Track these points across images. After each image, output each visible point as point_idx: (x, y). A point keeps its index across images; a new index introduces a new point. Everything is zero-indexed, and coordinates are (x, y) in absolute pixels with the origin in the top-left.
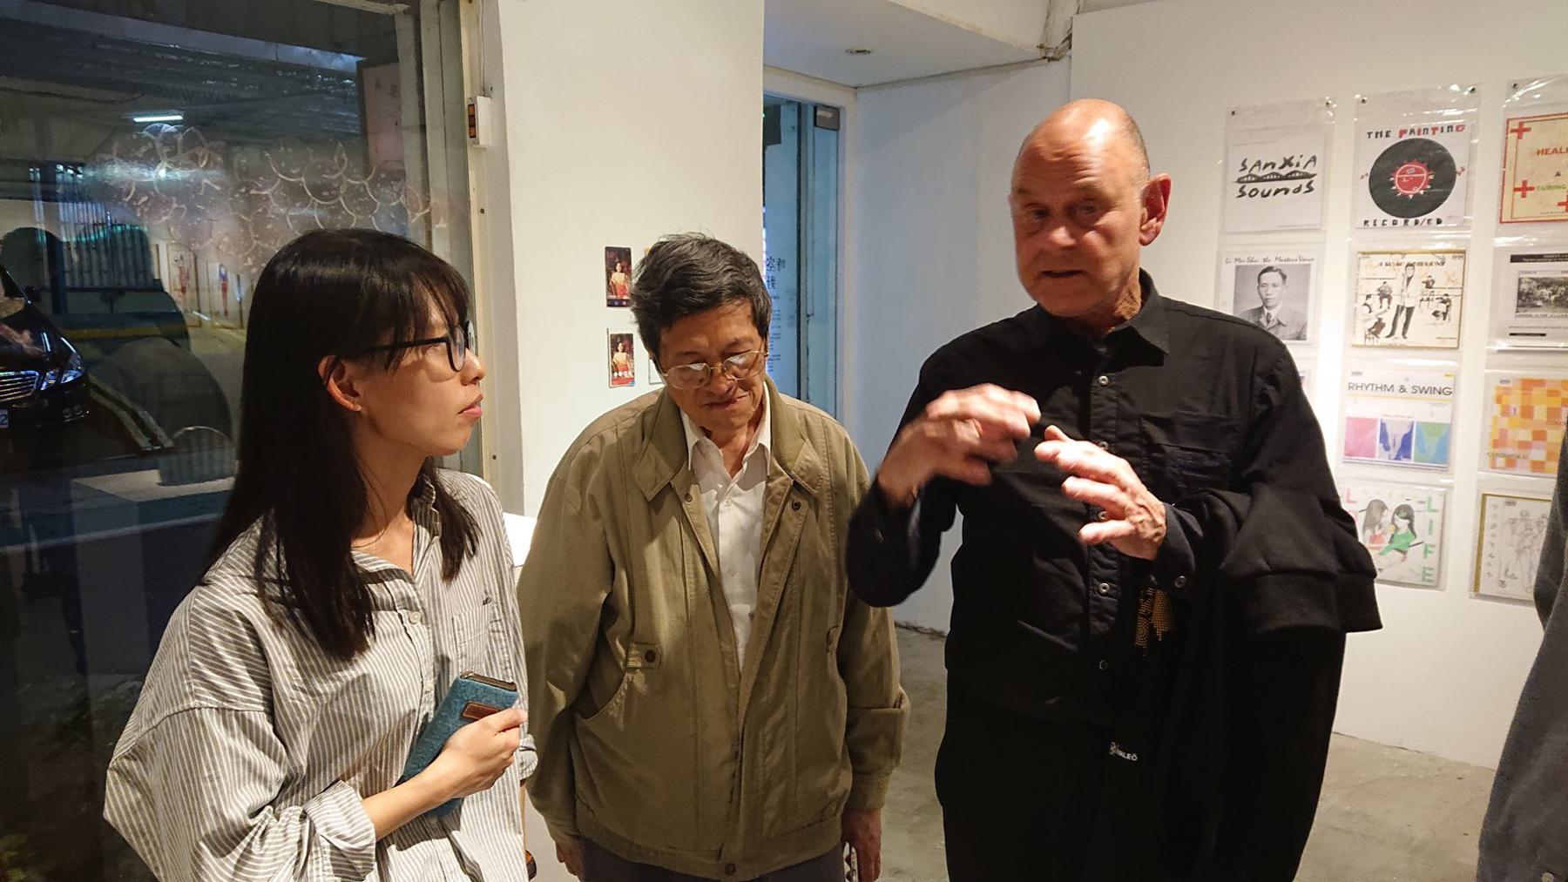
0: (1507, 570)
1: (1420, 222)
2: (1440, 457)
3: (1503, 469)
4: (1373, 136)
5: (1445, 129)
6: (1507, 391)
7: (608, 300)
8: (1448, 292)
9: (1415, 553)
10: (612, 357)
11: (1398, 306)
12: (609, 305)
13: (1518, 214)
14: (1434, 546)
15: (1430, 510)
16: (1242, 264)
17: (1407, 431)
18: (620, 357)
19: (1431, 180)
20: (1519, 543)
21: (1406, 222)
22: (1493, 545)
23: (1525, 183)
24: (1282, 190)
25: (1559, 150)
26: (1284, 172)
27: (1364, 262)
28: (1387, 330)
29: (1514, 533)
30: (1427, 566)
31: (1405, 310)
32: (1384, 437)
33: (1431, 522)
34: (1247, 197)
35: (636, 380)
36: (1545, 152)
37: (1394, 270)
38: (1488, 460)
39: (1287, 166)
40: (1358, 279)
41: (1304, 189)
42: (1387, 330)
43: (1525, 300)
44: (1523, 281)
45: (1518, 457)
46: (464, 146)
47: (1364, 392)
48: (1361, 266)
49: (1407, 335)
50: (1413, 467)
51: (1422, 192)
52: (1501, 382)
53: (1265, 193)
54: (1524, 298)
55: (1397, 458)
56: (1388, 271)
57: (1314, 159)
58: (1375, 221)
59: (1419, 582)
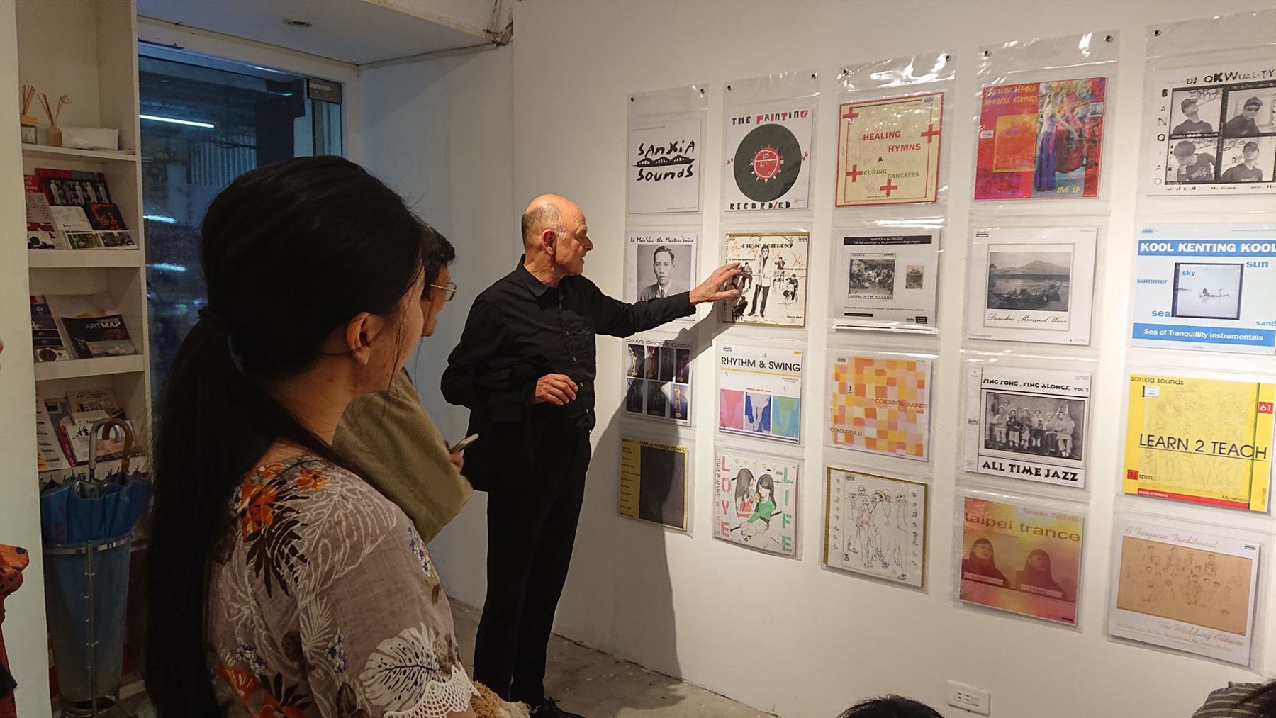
0: (849, 545)
2: (794, 434)
4: (737, 121)
5: (793, 115)
6: (844, 369)
11: (757, 285)
13: (852, 198)
16: (642, 243)
17: (766, 404)
20: (858, 518)
21: (763, 205)
23: (855, 167)
24: (669, 174)
26: (671, 157)
27: (731, 243)
31: (762, 289)
33: (787, 492)
36: (869, 137)
37: (753, 251)
38: (831, 437)
39: (673, 151)
41: (686, 173)
42: (748, 309)
43: (856, 281)
44: (854, 263)
50: (770, 439)
52: (839, 360)
53: (658, 177)
54: (854, 280)
57: (693, 143)
58: (739, 204)
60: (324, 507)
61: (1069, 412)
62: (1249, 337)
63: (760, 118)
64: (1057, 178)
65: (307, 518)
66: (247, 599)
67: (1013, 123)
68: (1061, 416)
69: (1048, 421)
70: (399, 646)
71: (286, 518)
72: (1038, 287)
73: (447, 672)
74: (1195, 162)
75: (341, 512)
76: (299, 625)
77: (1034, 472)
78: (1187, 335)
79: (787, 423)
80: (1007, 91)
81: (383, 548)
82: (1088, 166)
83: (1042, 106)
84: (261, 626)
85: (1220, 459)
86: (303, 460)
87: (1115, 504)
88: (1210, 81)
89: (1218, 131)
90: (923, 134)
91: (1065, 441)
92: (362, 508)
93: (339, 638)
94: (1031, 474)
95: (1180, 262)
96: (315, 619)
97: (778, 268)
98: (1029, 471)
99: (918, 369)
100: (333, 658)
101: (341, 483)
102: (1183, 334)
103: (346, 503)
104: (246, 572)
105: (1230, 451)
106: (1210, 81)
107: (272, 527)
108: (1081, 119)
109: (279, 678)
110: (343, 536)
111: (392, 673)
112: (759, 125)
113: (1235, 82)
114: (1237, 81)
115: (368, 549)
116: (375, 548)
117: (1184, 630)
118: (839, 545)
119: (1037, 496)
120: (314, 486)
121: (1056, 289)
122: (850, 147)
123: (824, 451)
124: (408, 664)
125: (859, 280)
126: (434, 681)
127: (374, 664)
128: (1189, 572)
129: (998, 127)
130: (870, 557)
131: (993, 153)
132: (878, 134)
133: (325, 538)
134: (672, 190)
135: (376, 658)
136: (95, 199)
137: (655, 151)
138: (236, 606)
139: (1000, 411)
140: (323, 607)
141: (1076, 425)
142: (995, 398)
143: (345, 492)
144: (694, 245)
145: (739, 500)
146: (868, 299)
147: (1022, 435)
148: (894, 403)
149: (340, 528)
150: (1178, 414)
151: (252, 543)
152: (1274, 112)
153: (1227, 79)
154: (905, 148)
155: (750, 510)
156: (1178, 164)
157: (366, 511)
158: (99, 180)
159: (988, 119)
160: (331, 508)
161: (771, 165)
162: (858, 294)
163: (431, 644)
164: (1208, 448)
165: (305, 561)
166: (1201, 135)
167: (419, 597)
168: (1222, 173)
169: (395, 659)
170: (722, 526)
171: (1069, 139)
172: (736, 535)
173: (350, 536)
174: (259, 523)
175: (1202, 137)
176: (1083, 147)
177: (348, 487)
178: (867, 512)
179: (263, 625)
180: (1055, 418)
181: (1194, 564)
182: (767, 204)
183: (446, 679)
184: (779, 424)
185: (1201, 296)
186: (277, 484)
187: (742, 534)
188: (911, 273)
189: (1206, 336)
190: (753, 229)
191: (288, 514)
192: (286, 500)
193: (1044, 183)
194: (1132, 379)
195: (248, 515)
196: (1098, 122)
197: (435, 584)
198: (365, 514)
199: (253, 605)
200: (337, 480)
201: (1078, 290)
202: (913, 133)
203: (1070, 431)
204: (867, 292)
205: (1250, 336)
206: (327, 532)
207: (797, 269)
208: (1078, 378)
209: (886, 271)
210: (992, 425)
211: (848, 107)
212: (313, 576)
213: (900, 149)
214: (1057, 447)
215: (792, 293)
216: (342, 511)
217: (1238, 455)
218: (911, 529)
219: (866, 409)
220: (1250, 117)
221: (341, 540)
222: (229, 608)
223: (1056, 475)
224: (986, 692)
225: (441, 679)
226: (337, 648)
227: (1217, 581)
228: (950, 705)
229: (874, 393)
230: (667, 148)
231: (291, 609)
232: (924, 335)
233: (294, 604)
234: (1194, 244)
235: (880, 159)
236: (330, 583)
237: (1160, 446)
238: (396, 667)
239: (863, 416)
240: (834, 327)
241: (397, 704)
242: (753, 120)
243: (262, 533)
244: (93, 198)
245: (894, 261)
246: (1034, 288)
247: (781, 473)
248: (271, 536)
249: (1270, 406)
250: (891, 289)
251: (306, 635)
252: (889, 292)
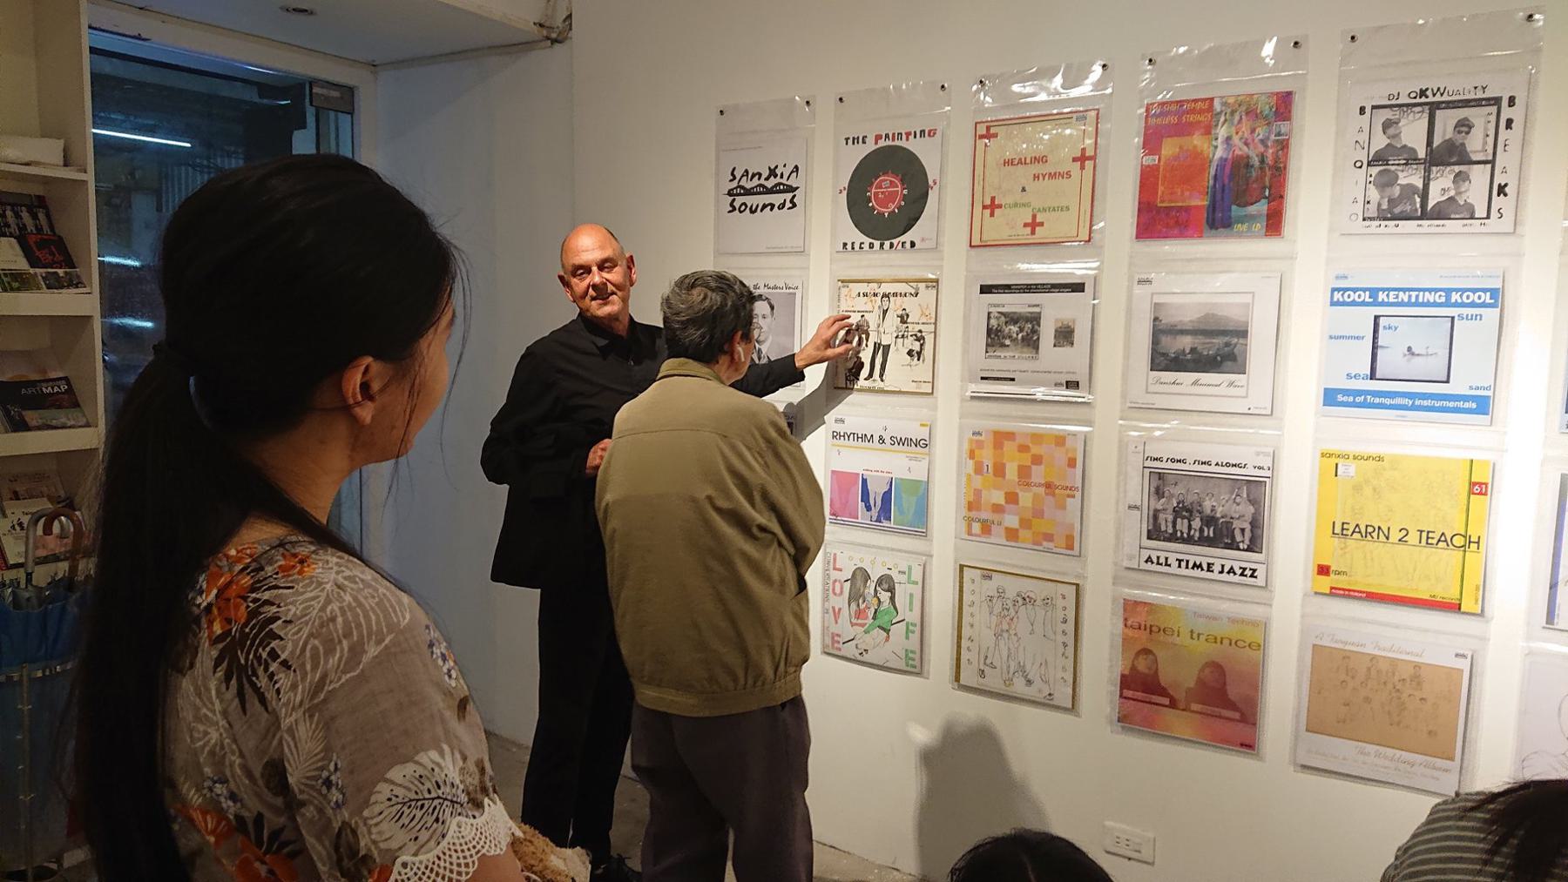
0: (986, 659)
2: (919, 524)
3: (979, 536)
4: (850, 141)
5: (918, 135)
6: (980, 445)
9: (898, 631)
11: (875, 343)
13: (989, 236)
14: (915, 625)
21: (882, 245)
23: (993, 199)
25: (1023, 160)
26: (769, 184)
27: (844, 291)
30: (910, 648)
33: (911, 595)
36: (1009, 163)
37: (871, 301)
38: (964, 529)
41: (788, 205)
42: (865, 372)
43: (995, 338)
44: (992, 315)
48: (842, 296)
53: (754, 208)
54: (993, 336)
55: (878, 520)
57: (796, 167)
58: (853, 243)
59: (902, 665)
60: (313, 599)
61: (1248, 495)
62: (1460, 404)
63: (878, 138)
64: (1233, 214)
65: (292, 613)
66: (215, 718)
67: (1181, 148)
68: (1238, 499)
69: (1223, 506)
70: (415, 774)
71: (264, 613)
72: (1210, 345)
73: (479, 805)
74: (1397, 195)
75: (335, 606)
76: (283, 750)
77: (1205, 567)
78: (1388, 401)
79: (912, 510)
80: (1174, 108)
81: (393, 650)
82: (1270, 199)
83: (1217, 125)
84: (233, 753)
85: (1427, 550)
86: (286, 541)
87: (1303, 606)
88: (1415, 98)
89: (1424, 157)
90: (1075, 160)
91: (1243, 530)
92: (362, 600)
93: (336, 765)
94: (1202, 570)
95: (1381, 314)
96: (303, 742)
97: (901, 322)
98: (1200, 566)
99: (1069, 443)
100: (328, 792)
101: (335, 568)
102: (1383, 400)
103: (342, 594)
104: (213, 685)
105: (1439, 541)
106: (1415, 98)
107: (246, 625)
108: (1263, 142)
109: (259, 818)
110: (338, 636)
111: (405, 808)
112: (875, 147)
113: (1443, 99)
114: (1445, 98)
115: (372, 651)
116: (381, 651)
117: (1386, 757)
118: (973, 656)
119: (1211, 597)
120: (300, 573)
121: (1232, 347)
122: (987, 174)
123: (955, 544)
124: (427, 796)
125: (998, 337)
126: (460, 818)
127: (382, 797)
128: (1392, 686)
129: (1163, 152)
130: (1011, 673)
131: (1158, 184)
132: (1020, 159)
133: (315, 638)
134: (769, 226)
135: (384, 790)
136: (34, 229)
137: (750, 176)
138: (201, 728)
139: (1166, 495)
140: (313, 726)
141: (1256, 509)
142: (1160, 479)
143: (342, 580)
145: (854, 606)
147: (1192, 523)
148: (1040, 485)
149: (335, 625)
150: (1377, 497)
151: (221, 646)
152: (1487, 136)
153: (1434, 95)
154: (1052, 176)
155: (866, 618)
156: (1379, 197)
157: (369, 604)
158: (38, 204)
159: (1151, 142)
160: (322, 600)
161: (891, 197)
163: (457, 772)
164: (1413, 538)
165: (289, 668)
166: (1404, 162)
167: (439, 711)
168: (1430, 206)
169: (409, 789)
170: (833, 638)
171: (1248, 166)
172: (850, 650)
173: (348, 635)
174: (229, 621)
175: (1406, 164)
176: (1265, 176)
177: (345, 574)
179: (237, 750)
180: (1231, 502)
181: (1396, 678)
182: (887, 244)
183: (477, 814)
184: (900, 511)
185: (1405, 355)
186: (252, 571)
187: (857, 648)
188: (1060, 328)
189: (1411, 403)
190: (870, 274)
191: (266, 608)
192: (263, 591)
193: (1218, 220)
194: (1323, 455)
195: (215, 611)
196: (1284, 145)
197: (462, 696)
198: (369, 608)
199: (223, 726)
200: (330, 565)
201: (1258, 349)
202: (1062, 159)
203: (1249, 518)
204: (1008, 351)
205: (1462, 403)
206: (317, 630)
207: (923, 323)
208: (1258, 454)
209: (1030, 326)
210: (1156, 512)
211: (986, 124)
212: (300, 687)
214: (1233, 538)
215: (917, 353)
216: (338, 604)
217: (1448, 545)
218: (1060, 638)
219: (1006, 493)
220: (1461, 141)
221: (336, 641)
222: (191, 730)
223: (1231, 571)
224: (1151, 835)
225: (470, 814)
226: (333, 778)
227: (1424, 697)
228: (1108, 852)
229: (1016, 474)
230: (763, 177)
231: (273, 729)
232: (1076, 403)
233: (276, 722)
234: (1396, 293)
235: (1024, 190)
236: (322, 696)
237: (1357, 536)
238: (411, 800)
239: (1002, 501)
240: (969, 394)
241: (413, 847)
242: (870, 140)
243: (233, 634)
244: (31, 227)
245: (1040, 313)
246: (1206, 346)
247: (904, 573)
248: (245, 636)
249: (1484, 486)
250: (1037, 348)
251: (292, 762)
252: (1034, 351)
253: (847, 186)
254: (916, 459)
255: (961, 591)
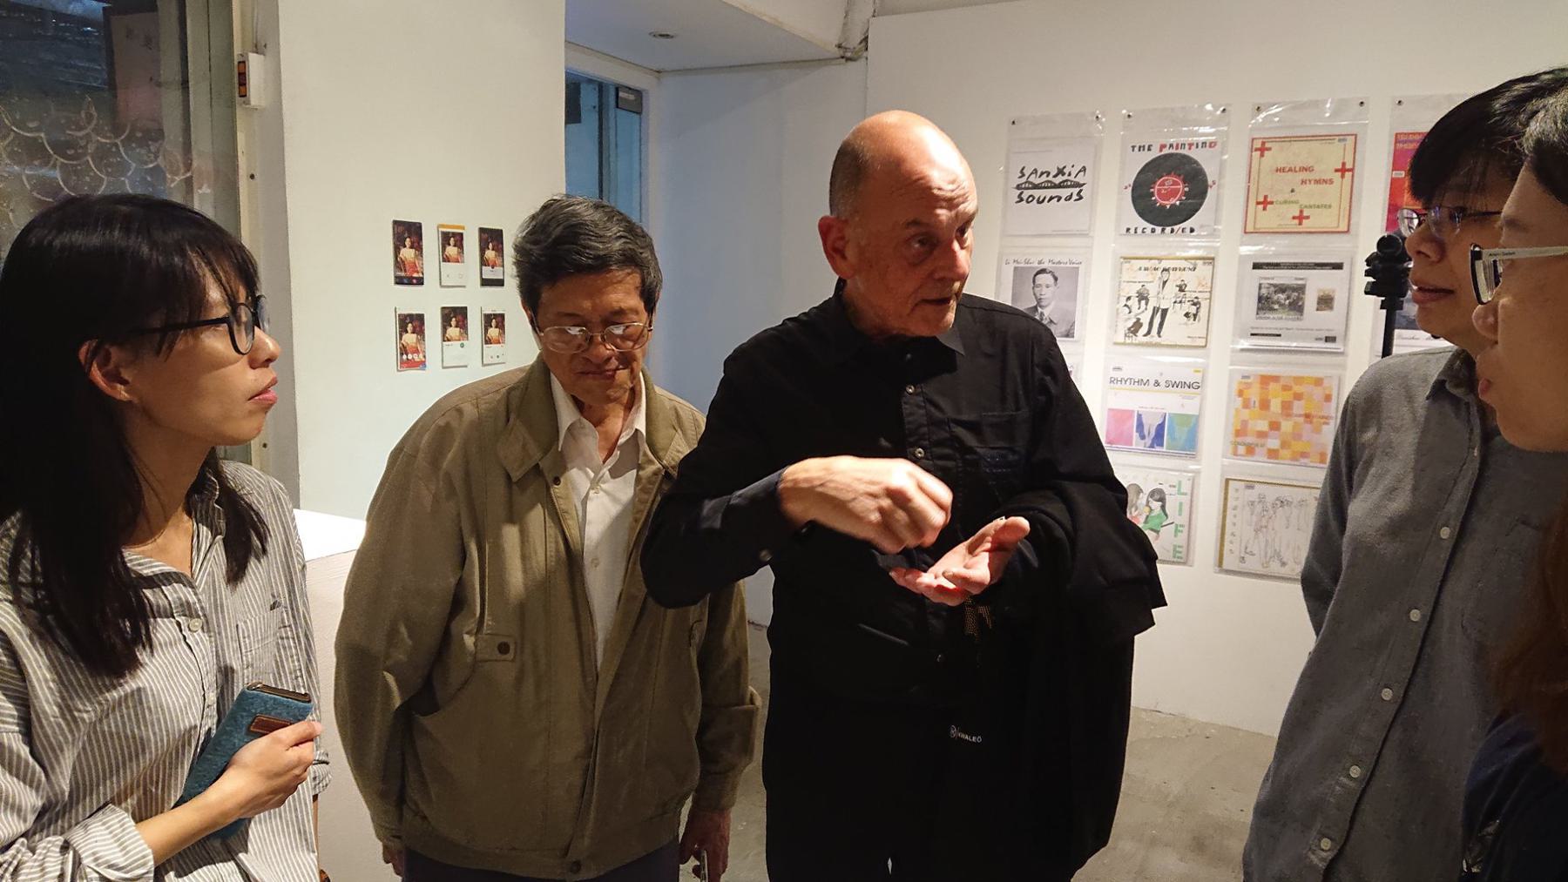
0: (1246, 548)
1: (1176, 231)
2: (1189, 446)
4: (1136, 149)
7: (396, 277)
8: (1196, 295)
10: (401, 339)
12: (397, 283)
13: (1262, 225)
15: (1180, 493)
16: (1019, 265)
18: (410, 338)
19: (1186, 192)
21: (1163, 230)
22: (1234, 524)
23: (1266, 197)
26: (1057, 180)
27: (1126, 266)
28: (1144, 329)
29: (1252, 514)
31: (1159, 314)
32: (1140, 426)
34: (1024, 202)
35: (427, 363)
36: (1282, 170)
39: (1060, 176)
40: (1120, 282)
41: (1075, 197)
42: (1144, 329)
43: (1265, 303)
45: (1257, 445)
46: (232, 106)
47: (1123, 386)
49: (1161, 334)
50: (1164, 455)
51: (1178, 203)
55: (1152, 446)
56: (1147, 275)
57: (1084, 169)
58: (1136, 229)
90: (1337, 171)
99: (1326, 383)
112: (1162, 153)
130: (1268, 558)
134: (1059, 213)
144: (1082, 267)
146: (1271, 322)
148: (1300, 416)
162: (1267, 315)
178: (1267, 517)
202: (1327, 168)
207: (1200, 292)
213: (1312, 182)
230: (1054, 172)
240: (1240, 347)
247: (1174, 486)
253: (1132, 183)
254: (1189, 398)
255: (1226, 499)
